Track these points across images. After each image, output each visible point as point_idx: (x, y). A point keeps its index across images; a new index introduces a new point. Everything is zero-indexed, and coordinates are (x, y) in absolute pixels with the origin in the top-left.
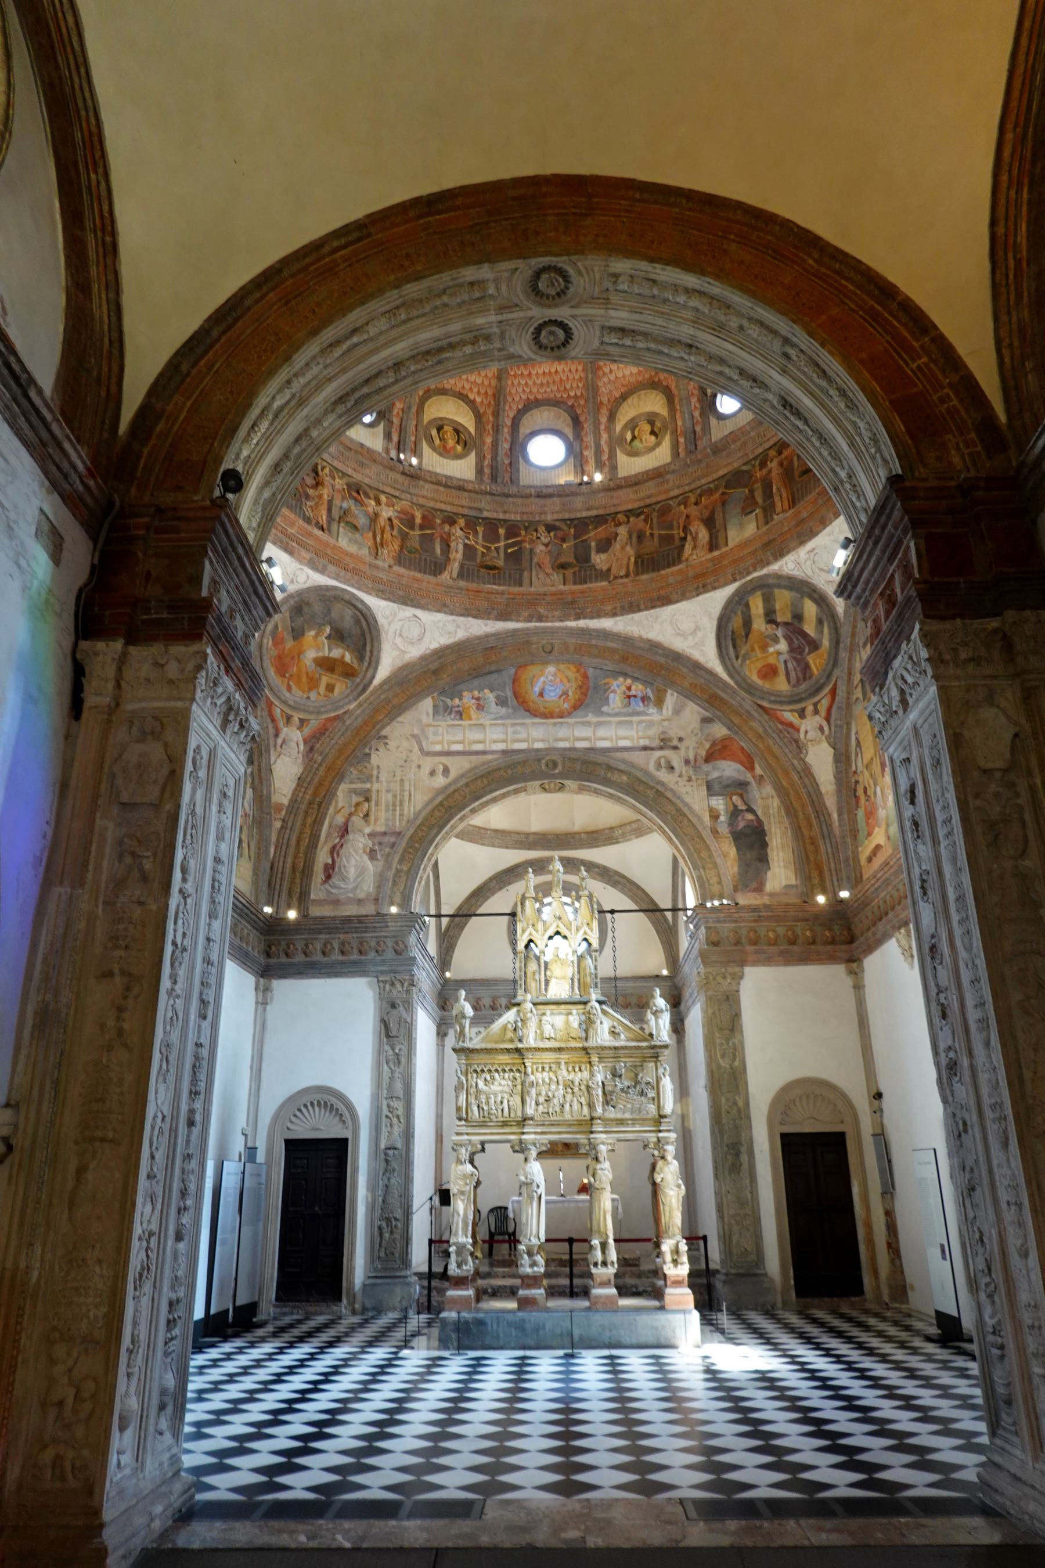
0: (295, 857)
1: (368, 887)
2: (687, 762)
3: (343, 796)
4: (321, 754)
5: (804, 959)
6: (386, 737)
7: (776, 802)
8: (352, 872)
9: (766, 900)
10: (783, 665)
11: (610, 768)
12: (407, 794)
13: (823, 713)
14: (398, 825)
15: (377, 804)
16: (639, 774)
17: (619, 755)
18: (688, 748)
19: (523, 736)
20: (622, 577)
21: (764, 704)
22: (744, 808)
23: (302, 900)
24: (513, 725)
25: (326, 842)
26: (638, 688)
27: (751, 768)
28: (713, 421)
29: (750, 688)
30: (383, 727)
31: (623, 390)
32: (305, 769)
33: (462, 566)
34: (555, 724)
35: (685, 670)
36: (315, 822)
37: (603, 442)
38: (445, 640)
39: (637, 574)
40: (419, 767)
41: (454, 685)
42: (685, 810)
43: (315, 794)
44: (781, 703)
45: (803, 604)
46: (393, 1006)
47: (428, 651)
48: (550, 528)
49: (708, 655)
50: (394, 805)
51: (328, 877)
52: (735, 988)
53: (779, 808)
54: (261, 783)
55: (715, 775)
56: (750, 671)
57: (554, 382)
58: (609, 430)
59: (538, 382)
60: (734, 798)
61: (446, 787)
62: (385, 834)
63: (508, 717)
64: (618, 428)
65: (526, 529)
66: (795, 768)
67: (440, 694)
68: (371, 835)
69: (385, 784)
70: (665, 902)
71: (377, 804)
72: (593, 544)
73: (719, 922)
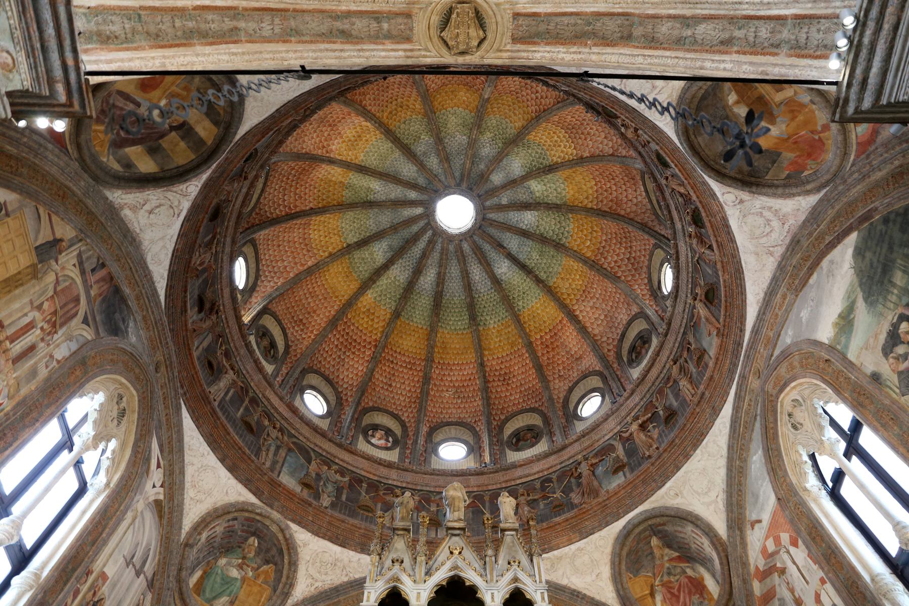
10: (139, 100)
45: (158, 164)
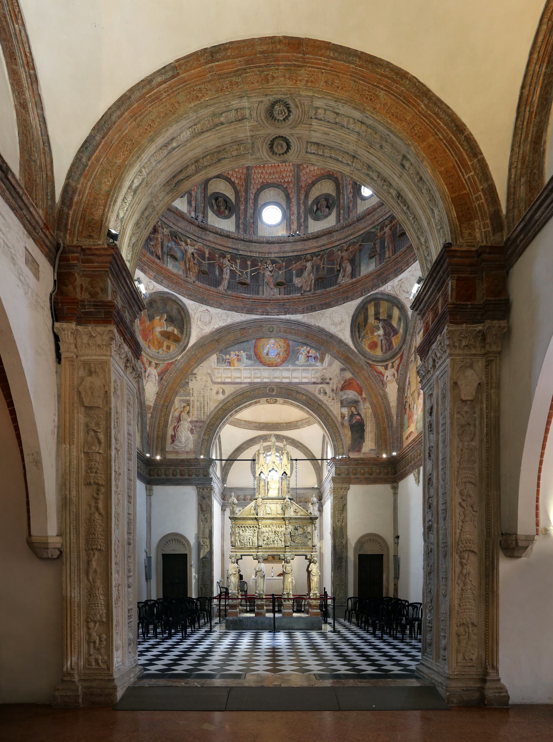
0: (158, 431)
1: (191, 446)
2: (333, 390)
3: (177, 403)
4: (166, 382)
5: (375, 481)
6: (195, 374)
7: (370, 411)
8: (183, 439)
9: (361, 456)
11: (298, 392)
12: (206, 402)
13: (396, 367)
14: (203, 418)
15: (193, 408)
16: (311, 396)
17: (302, 386)
18: (333, 383)
19: (259, 375)
20: (308, 291)
21: (370, 362)
22: (356, 413)
23: (163, 451)
24: (254, 369)
25: (171, 424)
26: (313, 352)
27: (361, 394)
28: (359, 201)
29: (364, 354)
30: (194, 369)
31: (314, 179)
32: (159, 389)
33: (229, 282)
34: (273, 370)
35: (335, 343)
36: (165, 414)
37: (301, 211)
38: (222, 324)
39: (315, 290)
40: (211, 389)
41: (227, 348)
42: (330, 414)
43: (164, 402)
44: (378, 362)
46: (204, 498)
47: (214, 330)
48: (273, 262)
49: (345, 336)
50: (201, 408)
51: (173, 441)
52: (345, 493)
53: (371, 414)
54: (140, 395)
55: (345, 397)
56: (365, 345)
57: (277, 172)
58: (305, 203)
59: (268, 172)
60: (352, 408)
61: (224, 400)
62: (197, 421)
63: (252, 365)
64: (310, 203)
65: (261, 261)
66: (380, 394)
67: (220, 352)
68: (191, 422)
69: (196, 397)
70: (318, 456)
71: (193, 408)
72: (294, 272)
73: (341, 465)
